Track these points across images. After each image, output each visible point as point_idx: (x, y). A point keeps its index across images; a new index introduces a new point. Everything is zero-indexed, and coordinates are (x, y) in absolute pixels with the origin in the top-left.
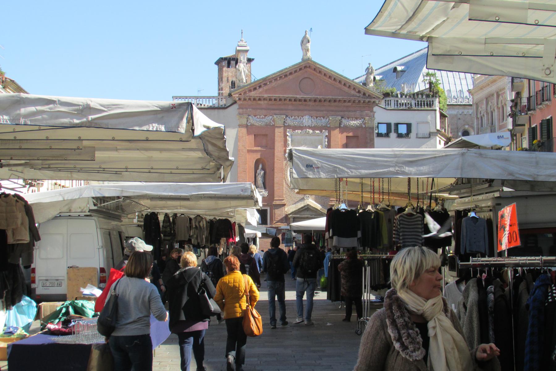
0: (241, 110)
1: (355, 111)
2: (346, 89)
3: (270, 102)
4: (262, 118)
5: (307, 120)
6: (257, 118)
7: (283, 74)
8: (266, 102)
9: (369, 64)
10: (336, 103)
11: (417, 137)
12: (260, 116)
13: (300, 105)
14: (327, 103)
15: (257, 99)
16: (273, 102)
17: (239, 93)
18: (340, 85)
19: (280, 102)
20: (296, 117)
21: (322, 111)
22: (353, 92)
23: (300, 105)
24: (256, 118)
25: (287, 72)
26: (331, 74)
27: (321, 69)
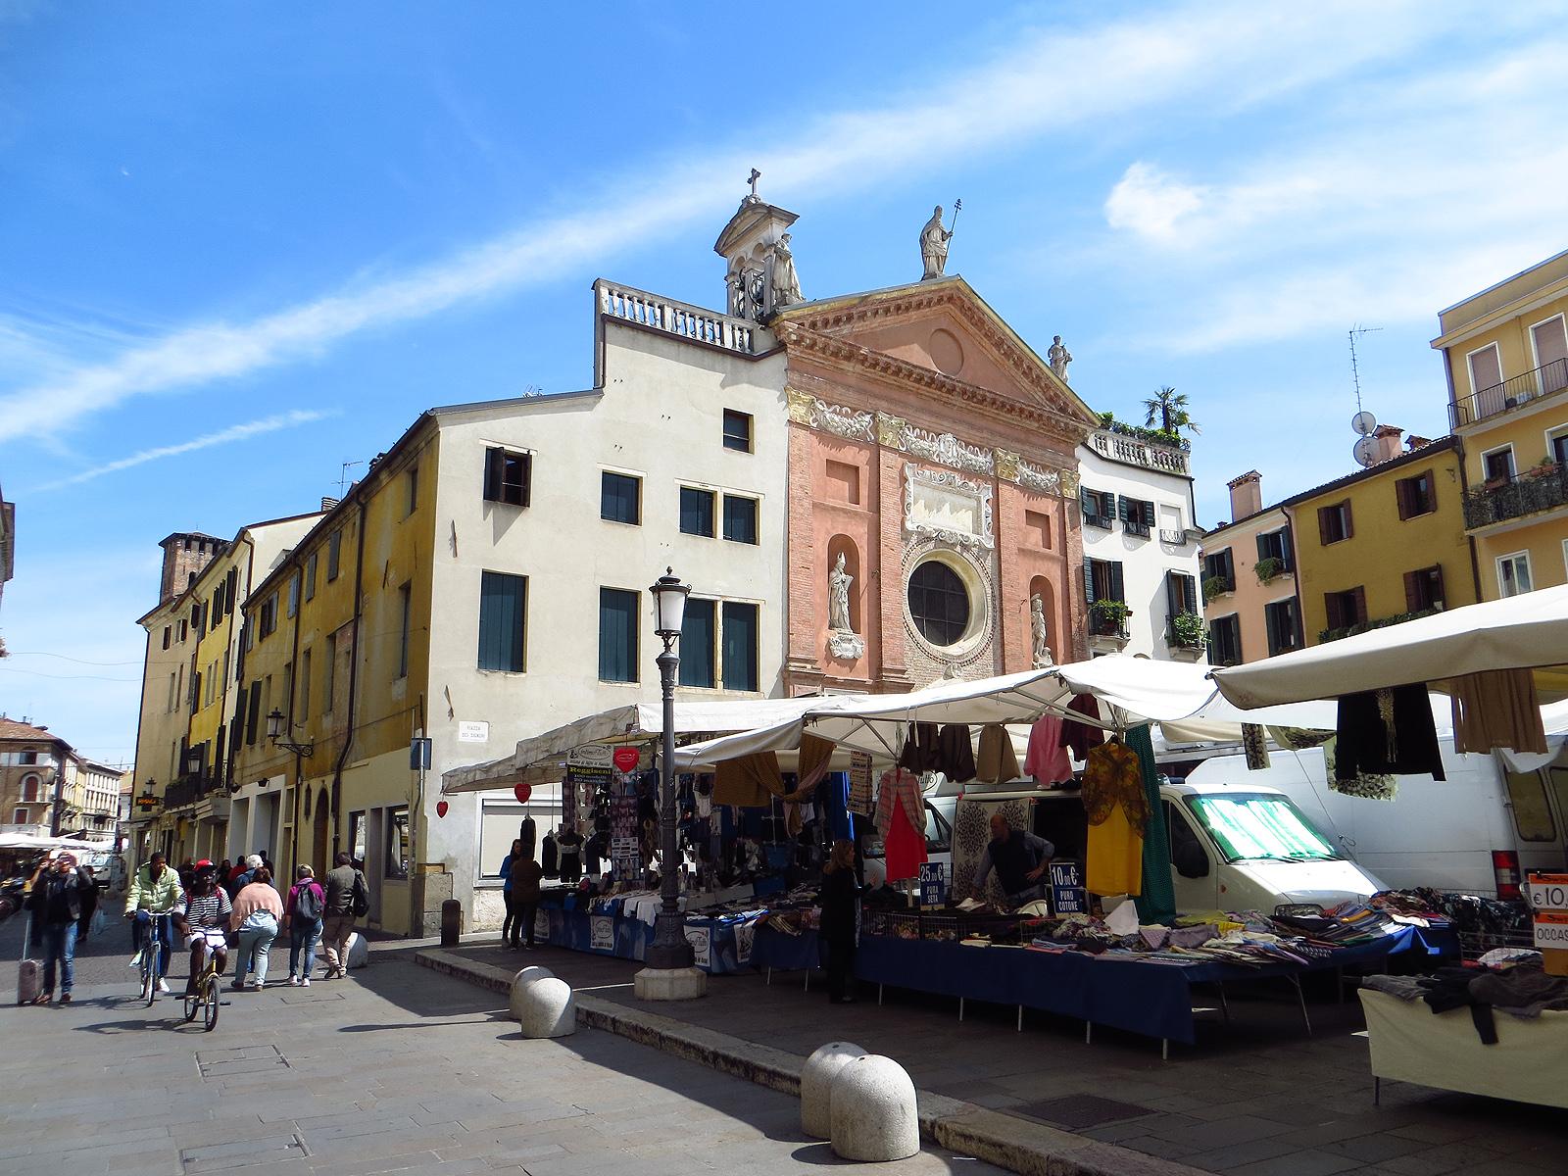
0: (796, 377)
1: (1044, 448)
2: (1025, 383)
3: (871, 373)
4: (846, 415)
5: (947, 448)
6: (834, 412)
7: (904, 297)
8: (859, 368)
9: (1056, 339)
10: (1009, 416)
11: (1161, 540)
12: (842, 407)
13: (935, 399)
14: (992, 411)
15: (845, 351)
16: (877, 373)
17: (799, 318)
18: (1014, 371)
19: (891, 379)
20: (924, 432)
21: (981, 429)
22: (1039, 396)
23: (935, 399)
24: (831, 410)
25: (912, 296)
26: (1004, 333)
27: (984, 313)
